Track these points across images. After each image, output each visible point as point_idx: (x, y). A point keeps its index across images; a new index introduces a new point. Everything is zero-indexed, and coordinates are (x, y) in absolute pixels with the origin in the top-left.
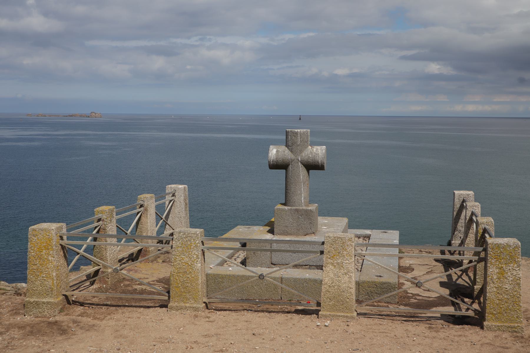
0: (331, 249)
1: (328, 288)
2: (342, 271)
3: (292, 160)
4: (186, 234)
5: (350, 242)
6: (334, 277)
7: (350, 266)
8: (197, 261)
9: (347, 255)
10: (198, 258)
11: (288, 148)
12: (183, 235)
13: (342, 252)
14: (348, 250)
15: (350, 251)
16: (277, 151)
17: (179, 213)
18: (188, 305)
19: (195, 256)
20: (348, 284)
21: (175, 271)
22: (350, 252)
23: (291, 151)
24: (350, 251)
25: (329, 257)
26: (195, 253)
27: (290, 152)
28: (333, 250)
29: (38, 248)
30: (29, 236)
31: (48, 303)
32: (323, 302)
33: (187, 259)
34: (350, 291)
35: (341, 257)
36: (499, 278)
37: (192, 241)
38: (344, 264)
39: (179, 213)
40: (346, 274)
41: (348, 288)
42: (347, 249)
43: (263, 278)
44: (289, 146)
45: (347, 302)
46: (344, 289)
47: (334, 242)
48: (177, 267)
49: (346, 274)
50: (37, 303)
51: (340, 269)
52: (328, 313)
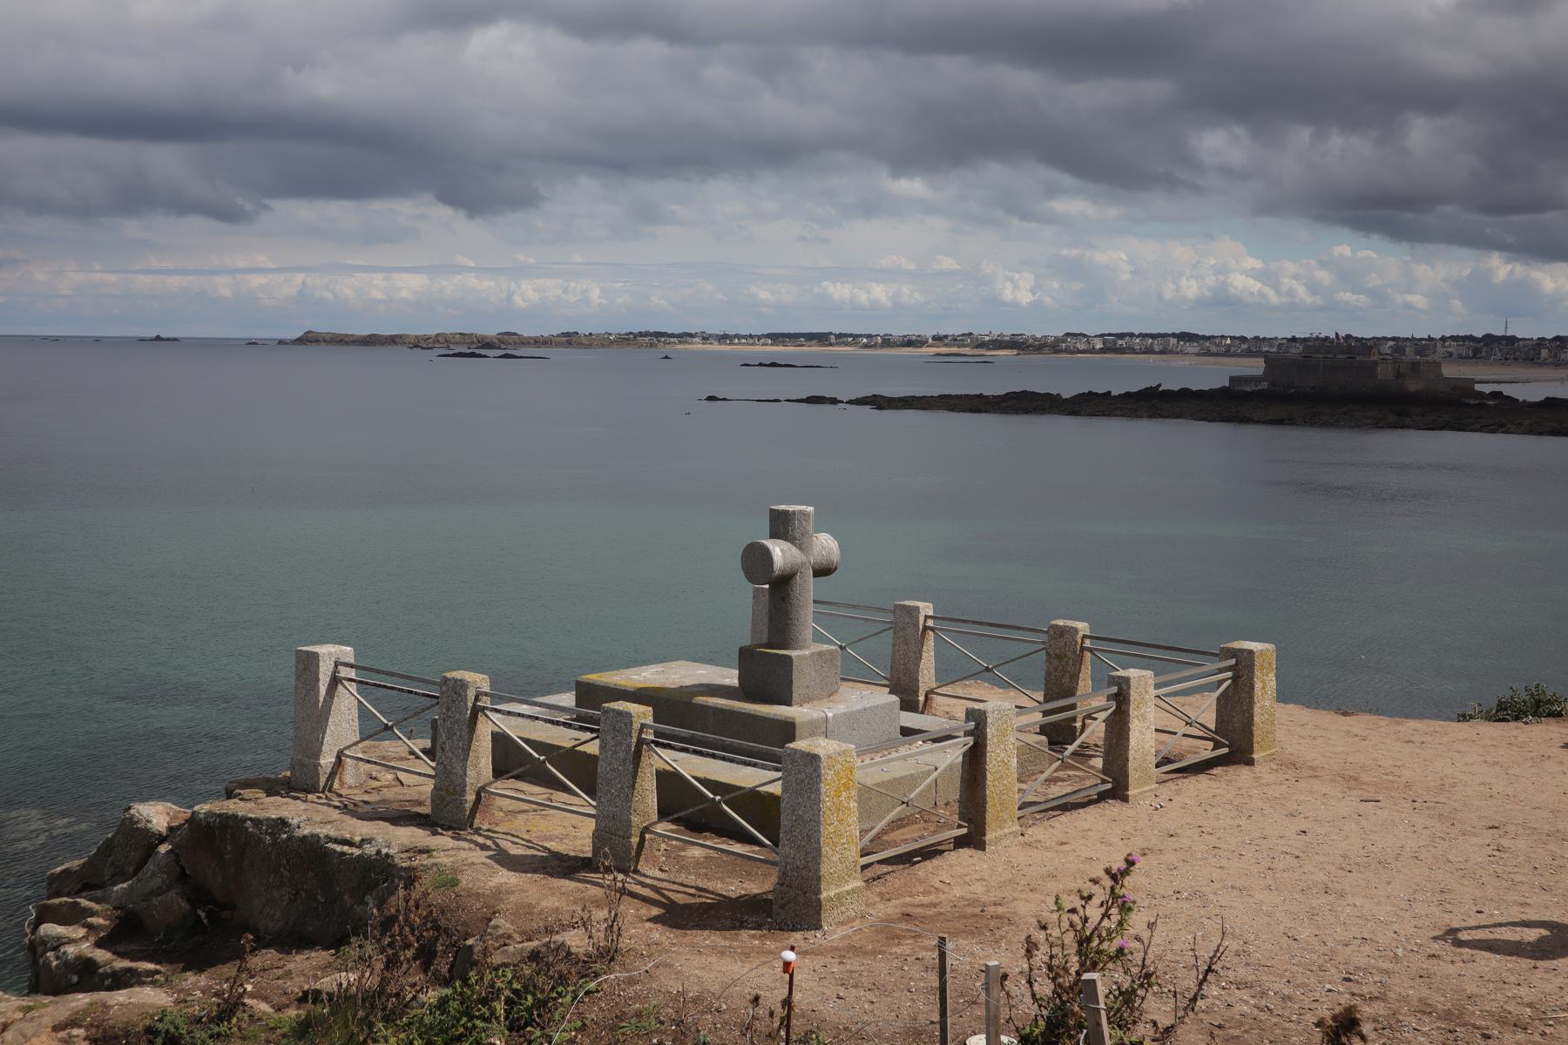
3: (803, 564)
11: (792, 543)
16: (782, 550)
17: (349, 709)
18: (1006, 831)
23: (800, 549)
27: (798, 552)
29: (836, 791)
30: (823, 771)
31: (853, 891)
33: (1002, 755)
39: (349, 709)
44: (795, 539)
50: (839, 897)
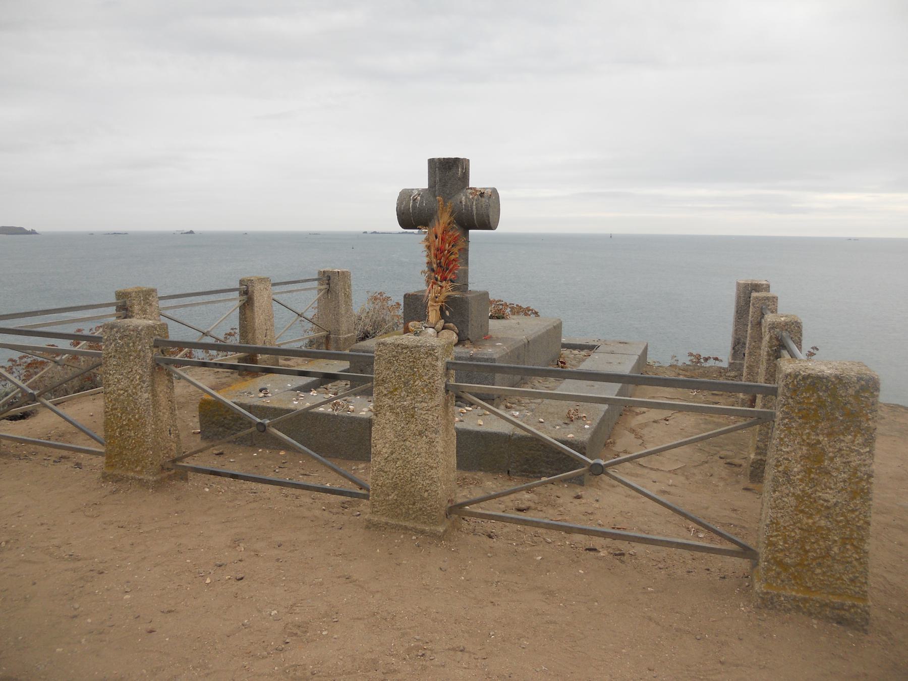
0: (388, 374)
1: (384, 464)
2: (413, 426)
4: (122, 330)
5: (430, 358)
6: (396, 440)
7: (431, 417)
8: (142, 387)
9: (423, 389)
10: (144, 382)
12: (117, 332)
13: (412, 382)
14: (425, 378)
15: (431, 381)
19: (138, 377)
20: (426, 459)
21: (109, 405)
22: (430, 383)
24: (431, 381)
25: (386, 392)
26: (136, 371)
28: (393, 376)
32: (373, 494)
34: (430, 474)
35: (410, 393)
36: (808, 471)
37: (131, 345)
38: (416, 409)
40: (421, 433)
41: (427, 468)
42: (423, 376)
43: (264, 429)
45: (423, 499)
46: (417, 467)
47: (394, 357)
48: (112, 396)
49: (421, 433)
51: (409, 421)
52: (384, 519)
